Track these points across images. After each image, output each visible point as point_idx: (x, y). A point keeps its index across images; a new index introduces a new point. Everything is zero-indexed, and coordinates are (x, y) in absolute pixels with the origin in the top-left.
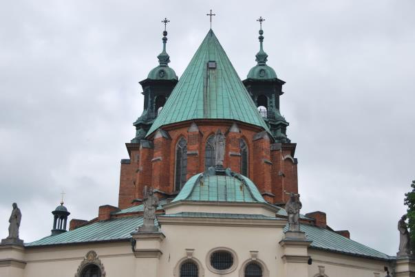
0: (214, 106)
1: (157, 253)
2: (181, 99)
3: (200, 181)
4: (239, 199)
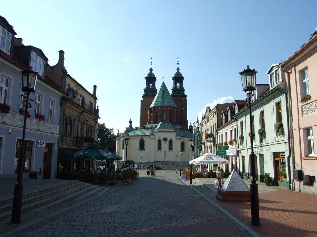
1: (154, 138)
3: (161, 124)
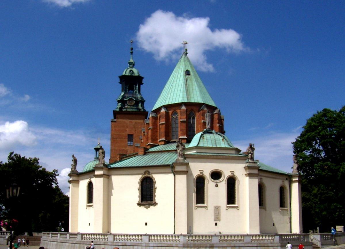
0: (192, 95)
2: (173, 90)
4: (223, 146)
